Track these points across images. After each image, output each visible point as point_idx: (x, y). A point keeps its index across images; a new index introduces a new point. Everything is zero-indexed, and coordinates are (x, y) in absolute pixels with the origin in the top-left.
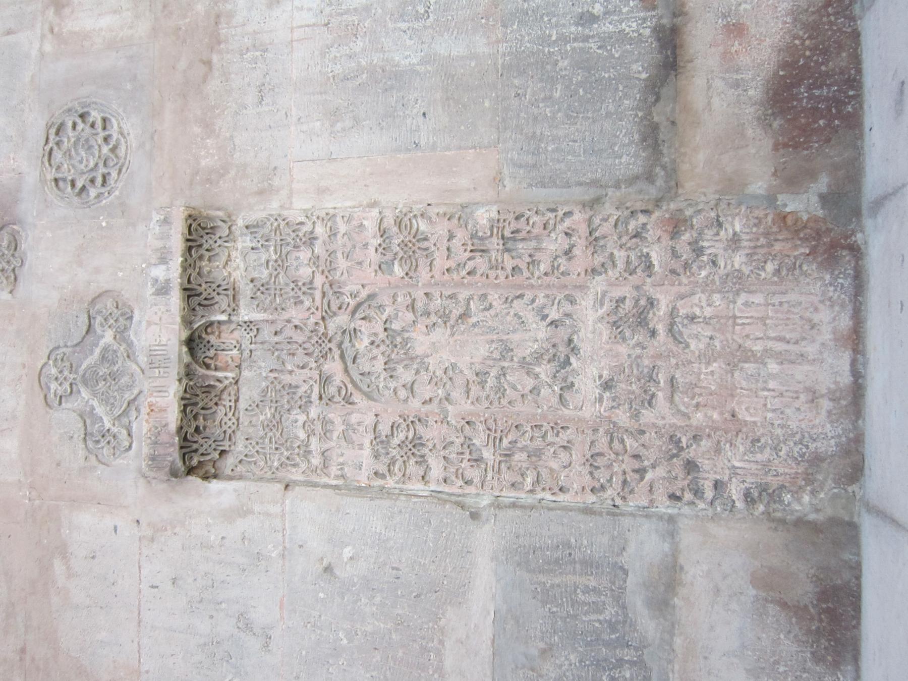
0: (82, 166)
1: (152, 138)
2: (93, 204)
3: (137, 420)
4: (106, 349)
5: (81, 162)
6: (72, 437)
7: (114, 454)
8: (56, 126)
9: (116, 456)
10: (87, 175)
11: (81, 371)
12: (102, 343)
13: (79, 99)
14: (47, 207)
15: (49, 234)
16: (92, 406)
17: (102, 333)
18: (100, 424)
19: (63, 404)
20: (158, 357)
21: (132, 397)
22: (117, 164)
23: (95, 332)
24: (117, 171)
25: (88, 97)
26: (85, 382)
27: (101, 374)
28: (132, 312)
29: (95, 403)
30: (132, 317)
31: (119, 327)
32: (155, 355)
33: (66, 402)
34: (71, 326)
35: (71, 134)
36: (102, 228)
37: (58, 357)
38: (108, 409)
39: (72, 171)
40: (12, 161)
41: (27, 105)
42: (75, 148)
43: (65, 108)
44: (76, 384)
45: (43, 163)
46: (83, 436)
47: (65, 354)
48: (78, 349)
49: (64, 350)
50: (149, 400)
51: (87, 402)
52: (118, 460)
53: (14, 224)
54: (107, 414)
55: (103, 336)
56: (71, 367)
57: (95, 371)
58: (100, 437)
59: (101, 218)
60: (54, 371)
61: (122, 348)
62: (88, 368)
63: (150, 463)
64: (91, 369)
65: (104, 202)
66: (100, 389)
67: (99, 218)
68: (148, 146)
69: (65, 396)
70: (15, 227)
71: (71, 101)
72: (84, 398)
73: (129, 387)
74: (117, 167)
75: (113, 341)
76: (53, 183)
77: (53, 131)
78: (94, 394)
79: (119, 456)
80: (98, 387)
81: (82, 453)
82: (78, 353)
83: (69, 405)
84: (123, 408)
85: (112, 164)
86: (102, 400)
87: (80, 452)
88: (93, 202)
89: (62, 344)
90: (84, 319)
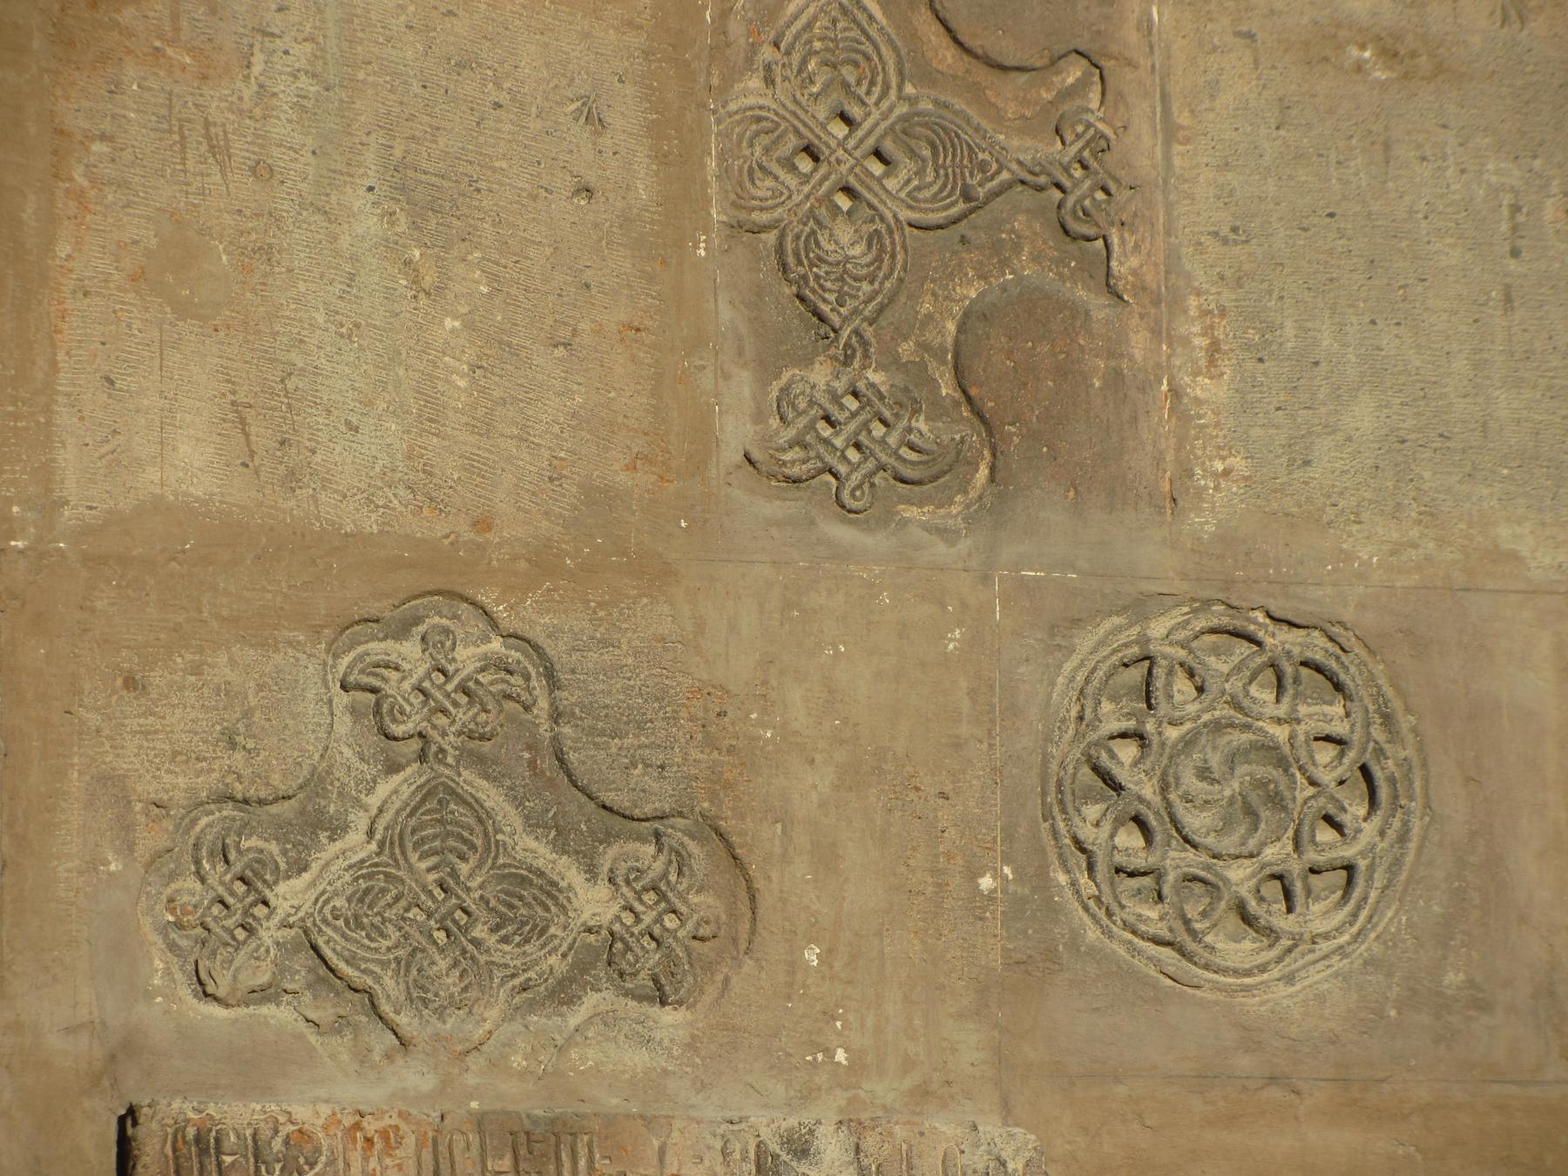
0: (1190, 782)
1: (1273, 1080)
2: (1055, 833)
3: (302, 1024)
4: (552, 892)
5: (1204, 773)
6: (233, 745)
7: (179, 925)
8: (1334, 665)
9: (173, 935)
10: (1157, 800)
11: (472, 782)
12: (570, 873)
13: (1424, 765)
14: (1053, 629)
15: (954, 640)
16: (345, 828)
17: (605, 866)
18: (283, 866)
19: (342, 699)
20: (552, 1167)
21: (386, 1008)
22: (1193, 933)
23: (609, 838)
24: (1168, 936)
25: (1427, 806)
26: (437, 795)
27: (464, 868)
28: (680, 1003)
29: (356, 843)
30: (663, 1003)
31: (628, 948)
32: (558, 1159)
33: (353, 710)
34: (627, 741)
35: (1301, 729)
36: (973, 874)
37: (516, 680)
38: (339, 902)
39: (1173, 733)
40: (1219, 466)
41: (1414, 533)
42: (1254, 747)
43: (1397, 705)
44: (422, 756)
45: (1207, 603)
46: (238, 790)
47: (527, 708)
48: (547, 763)
49: (543, 703)
50: (404, 1127)
51: (358, 803)
52: (159, 941)
53: (992, 478)
54: (322, 900)
55: (592, 873)
56: (482, 738)
57: (473, 847)
58: (237, 868)
59: (1007, 870)
60: (466, 657)
61: (553, 960)
62: (482, 816)
63: (191, 1132)
64: (478, 829)
65: (1062, 879)
66: (411, 868)
67: (1007, 859)
68: (1244, 1063)
69: (377, 711)
70: (983, 472)
71: (1415, 731)
72: (370, 791)
73: (420, 996)
74: (1184, 938)
75: (576, 924)
76: (1135, 650)
77: (1317, 646)
78: (396, 844)
79: (172, 947)
80: (414, 857)
81: (178, 784)
82: (532, 764)
83: (344, 724)
84: (342, 966)
85: (1192, 911)
86: (370, 876)
87: (181, 781)
88: (1061, 825)
89: (567, 698)
90: (658, 795)
